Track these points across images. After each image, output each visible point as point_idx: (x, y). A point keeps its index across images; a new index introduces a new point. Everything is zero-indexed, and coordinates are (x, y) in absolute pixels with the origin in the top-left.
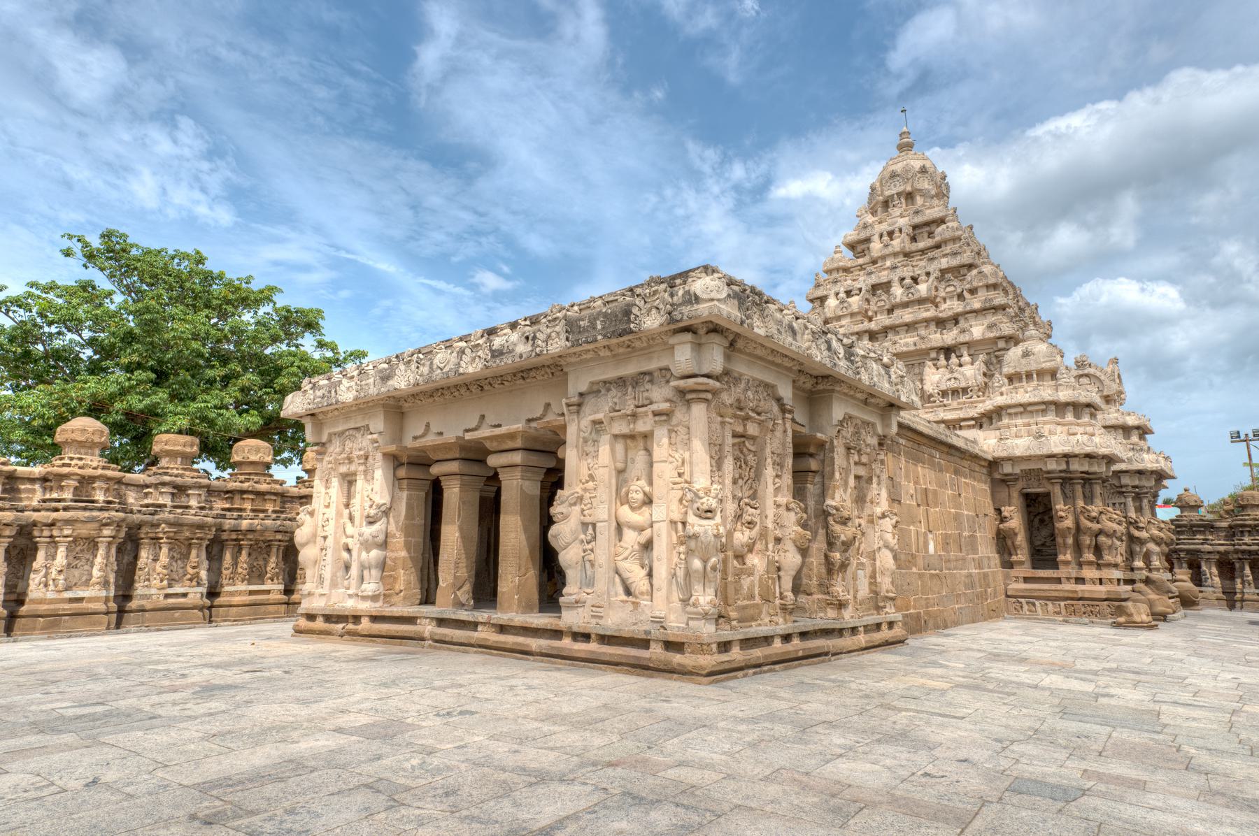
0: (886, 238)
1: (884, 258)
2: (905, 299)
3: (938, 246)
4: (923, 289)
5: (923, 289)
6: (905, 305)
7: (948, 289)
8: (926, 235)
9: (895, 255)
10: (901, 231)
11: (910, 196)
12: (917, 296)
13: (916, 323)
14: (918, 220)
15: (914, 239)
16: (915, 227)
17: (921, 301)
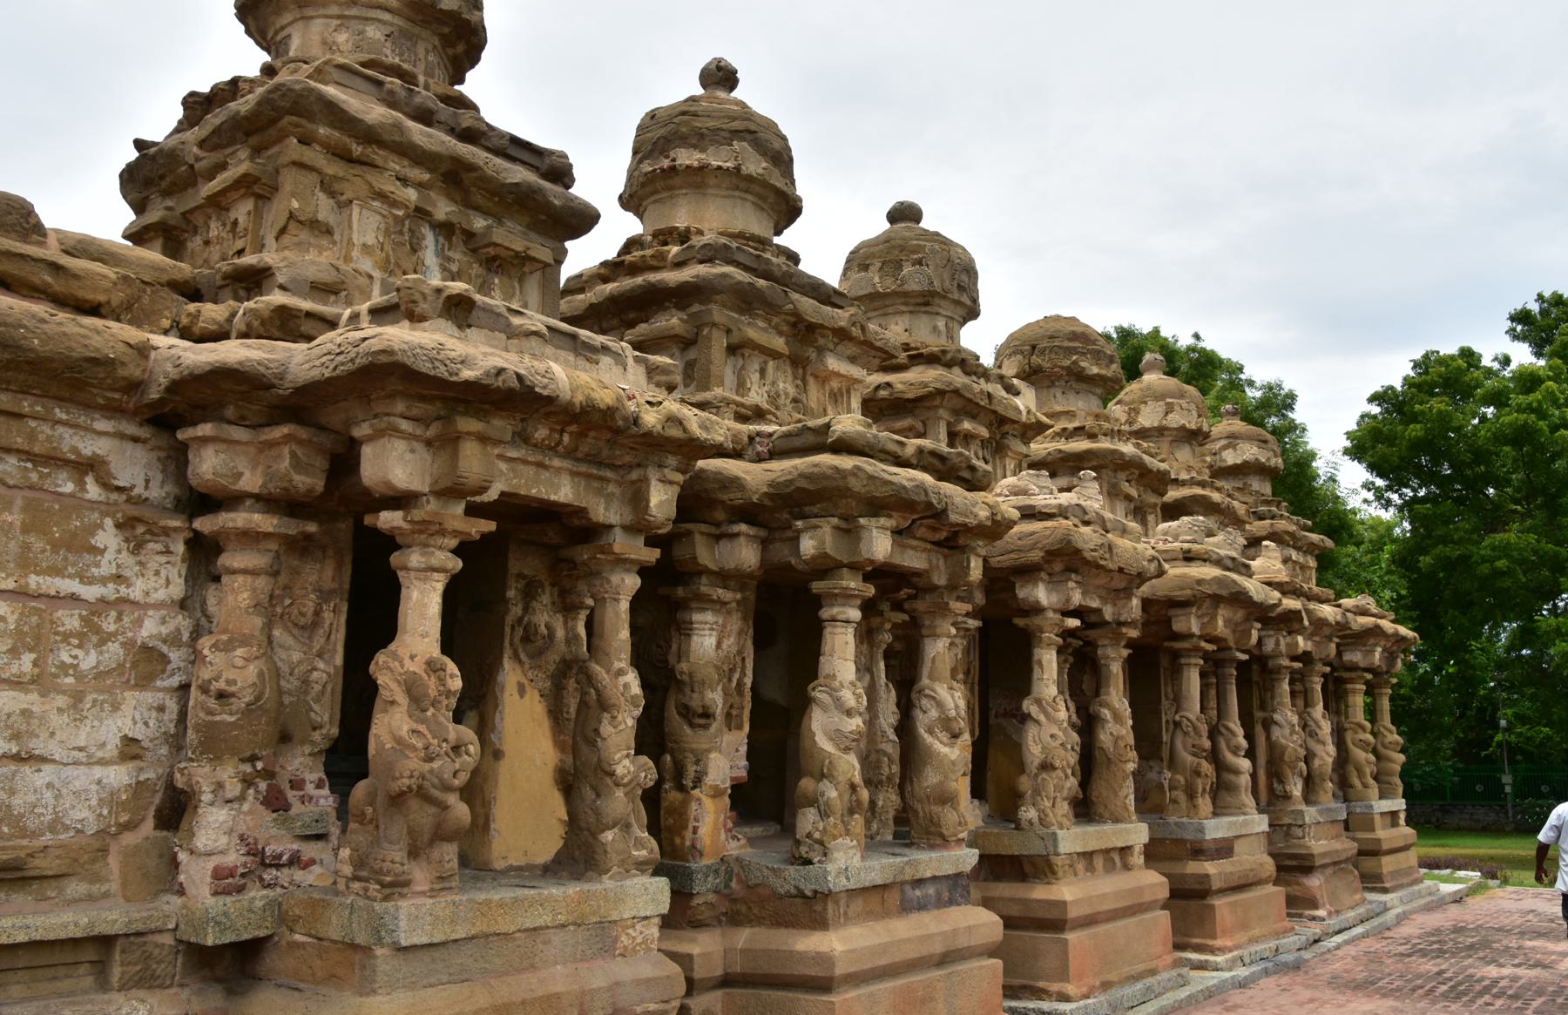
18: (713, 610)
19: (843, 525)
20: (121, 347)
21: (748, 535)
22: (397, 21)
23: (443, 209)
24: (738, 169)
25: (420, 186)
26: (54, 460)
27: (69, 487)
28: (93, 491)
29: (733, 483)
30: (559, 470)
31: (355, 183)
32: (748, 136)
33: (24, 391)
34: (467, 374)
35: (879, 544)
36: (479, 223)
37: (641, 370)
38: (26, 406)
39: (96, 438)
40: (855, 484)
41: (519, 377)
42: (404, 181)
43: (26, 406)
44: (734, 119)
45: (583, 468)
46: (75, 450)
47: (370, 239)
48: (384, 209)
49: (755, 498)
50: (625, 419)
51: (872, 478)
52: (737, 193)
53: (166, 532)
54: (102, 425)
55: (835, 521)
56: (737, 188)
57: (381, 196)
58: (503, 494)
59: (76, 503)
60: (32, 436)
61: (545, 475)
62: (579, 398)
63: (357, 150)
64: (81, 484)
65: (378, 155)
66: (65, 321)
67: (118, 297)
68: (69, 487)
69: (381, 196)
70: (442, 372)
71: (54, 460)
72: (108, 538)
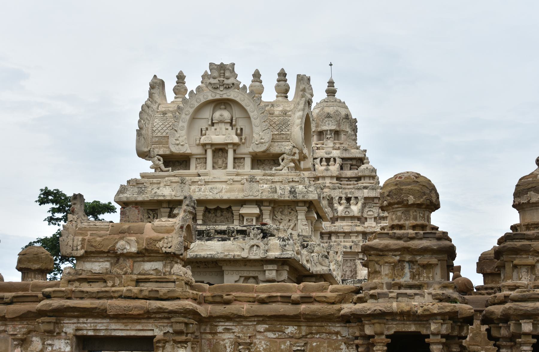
0: (324, 163)
1: (324, 177)
2: (343, 215)
3: (359, 179)
4: (355, 209)
5: (355, 209)
6: (343, 218)
7: (370, 213)
8: (349, 166)
9: (332, 177)
10: (335, 160)
11: (337, 133)
12: (351, 214)
13: (350, 233)
14: (346, 155)
15: (342, 168)
16: (343, 159)
17: (353, 218)
18: (506, 348)
19: (517, 322)
20: (335, 311)
21: (504, 327)
22: (404, 209)
23: (408, 257)
24: (529, 202)
25: (399, 255)
26: (330, 333)
27: (335, 338)
28: (340, 338)
29: (492, 313)
30: (410, 324)
31: (382, 260)
32: (533, 189)
33: (322, 322)
34: (369, 312)
35: (527, 327)
36: (418, 258)
37: (430, 296)
38: (323, 324)
39: (337, 328)
40: (511, 312)
41: (380, 310)
42: (396, 256)
43: (323, 324)
44: (529, 184)
45: (416, 323)
46: (334, 331)
47: (387, 272)
48: (389, 265)
49: (499, 317)
50: (413, 312)
51: (515, 309)
52: (533, 208)
53: (352, 344)
54: (337, 325)
55: (514, 322)
56: (533, 207)
57: (386, 262)
58: (395, 332)
59: (337, 341)
60: (326, 329)
61: (406, 326)
62: (399, 310)
63: (381, 253)
64: (337, 337)
65: (386, 253)
66: (330, 306)
67: (337, 300)
68: (335, 338)
69: (386, 262)
70: (363, 313)
71: (330, 333)
72: (343, 346)
